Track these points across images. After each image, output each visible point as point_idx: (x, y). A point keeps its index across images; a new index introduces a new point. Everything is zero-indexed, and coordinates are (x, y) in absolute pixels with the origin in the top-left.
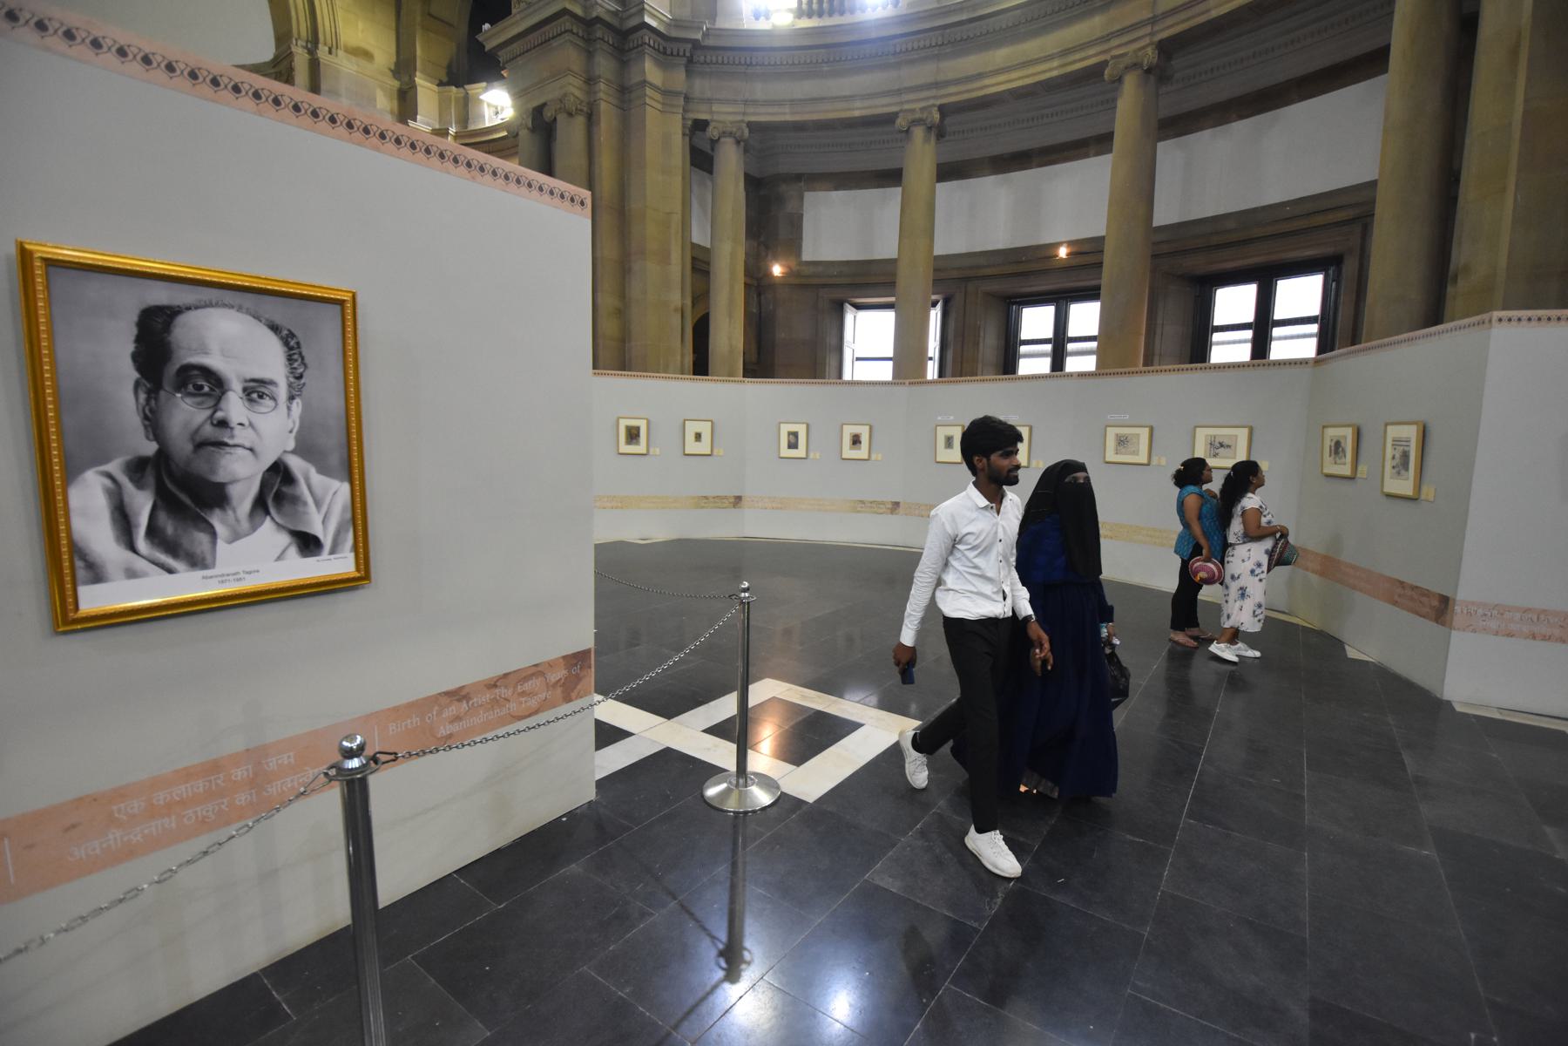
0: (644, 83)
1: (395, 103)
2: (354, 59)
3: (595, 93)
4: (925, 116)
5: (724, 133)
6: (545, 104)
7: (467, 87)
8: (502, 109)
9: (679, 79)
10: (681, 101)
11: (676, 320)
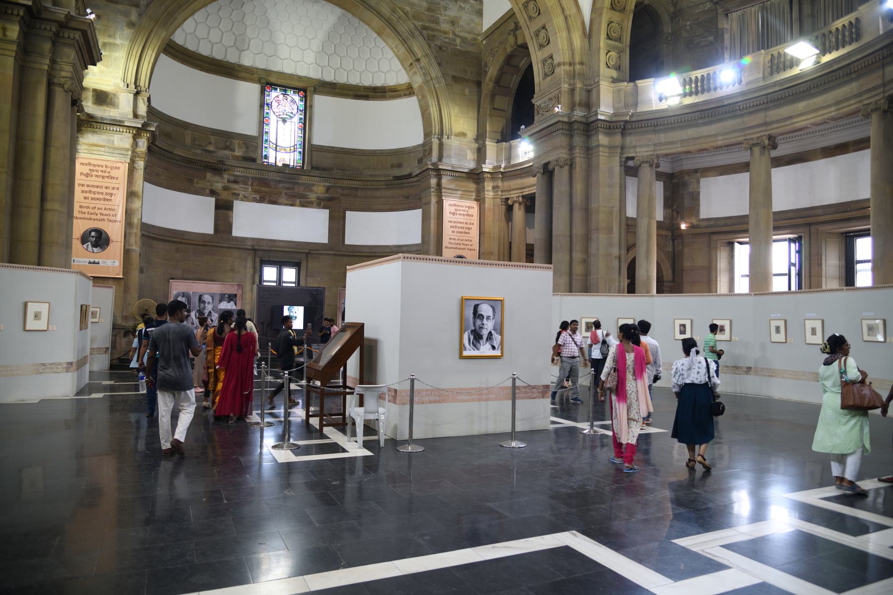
0: (598, 146)
1: (476, 155)
2: (458, 138)
3: (574, 154)
4: (759, 142)
5: (643, 162)
6: (549, 162)
7: (511, 142)
8: (529, 152)
9: (617, 139)
10: (619, 150)
11: (616, 263)
